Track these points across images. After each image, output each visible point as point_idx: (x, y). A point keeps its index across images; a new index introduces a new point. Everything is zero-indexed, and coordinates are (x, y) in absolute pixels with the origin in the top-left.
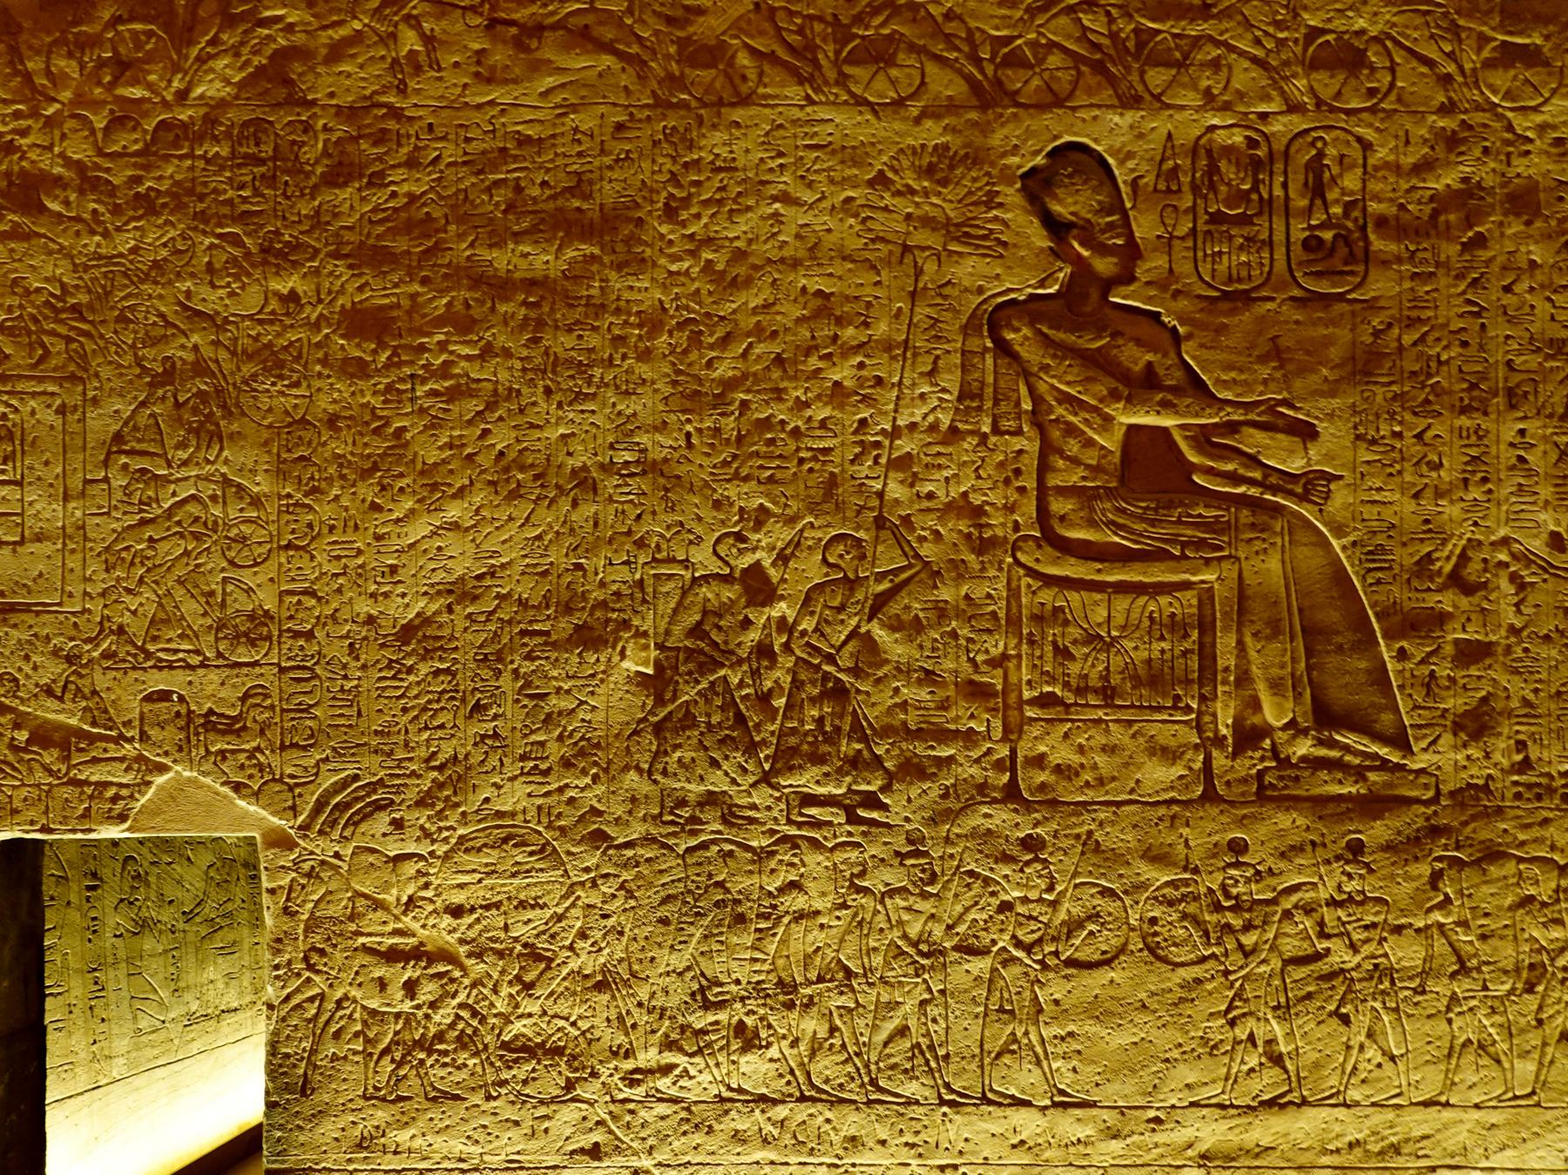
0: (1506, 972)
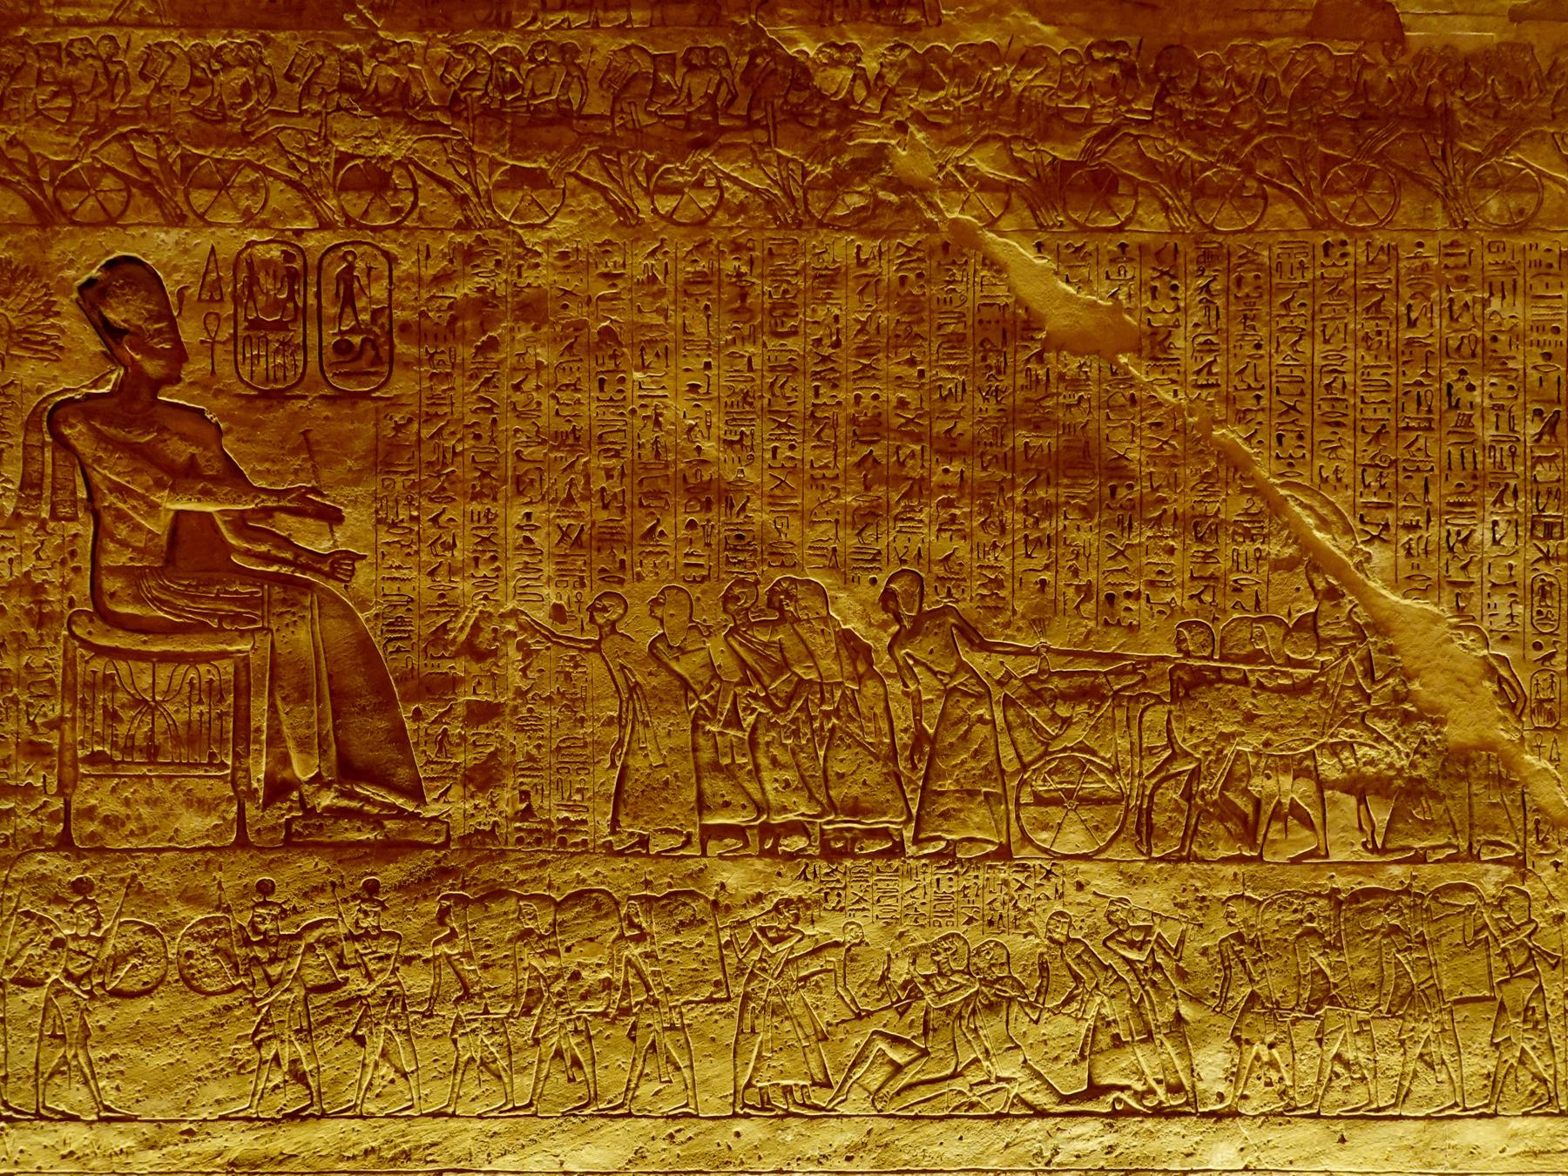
0: (505, 997)
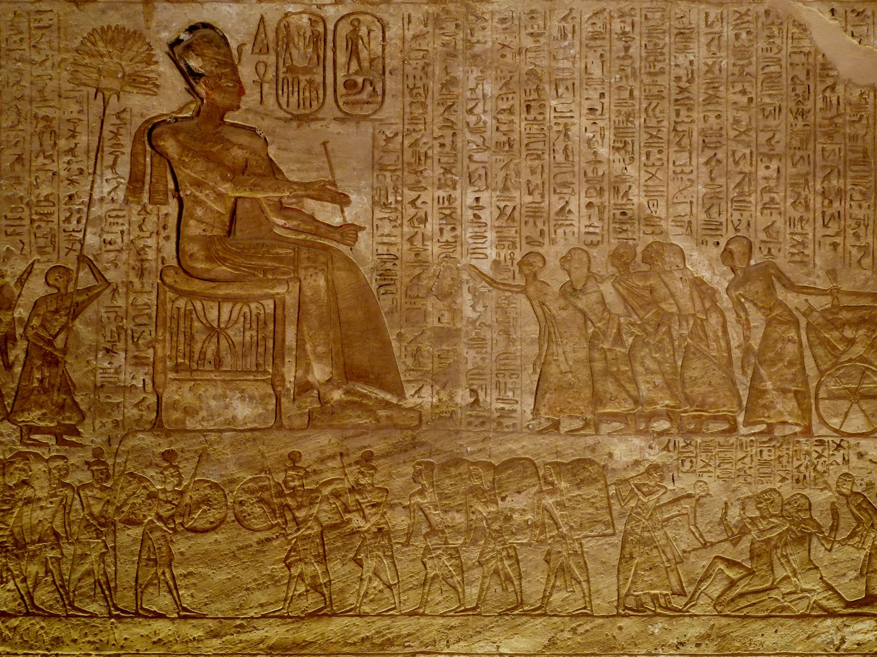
0: (459, 532)
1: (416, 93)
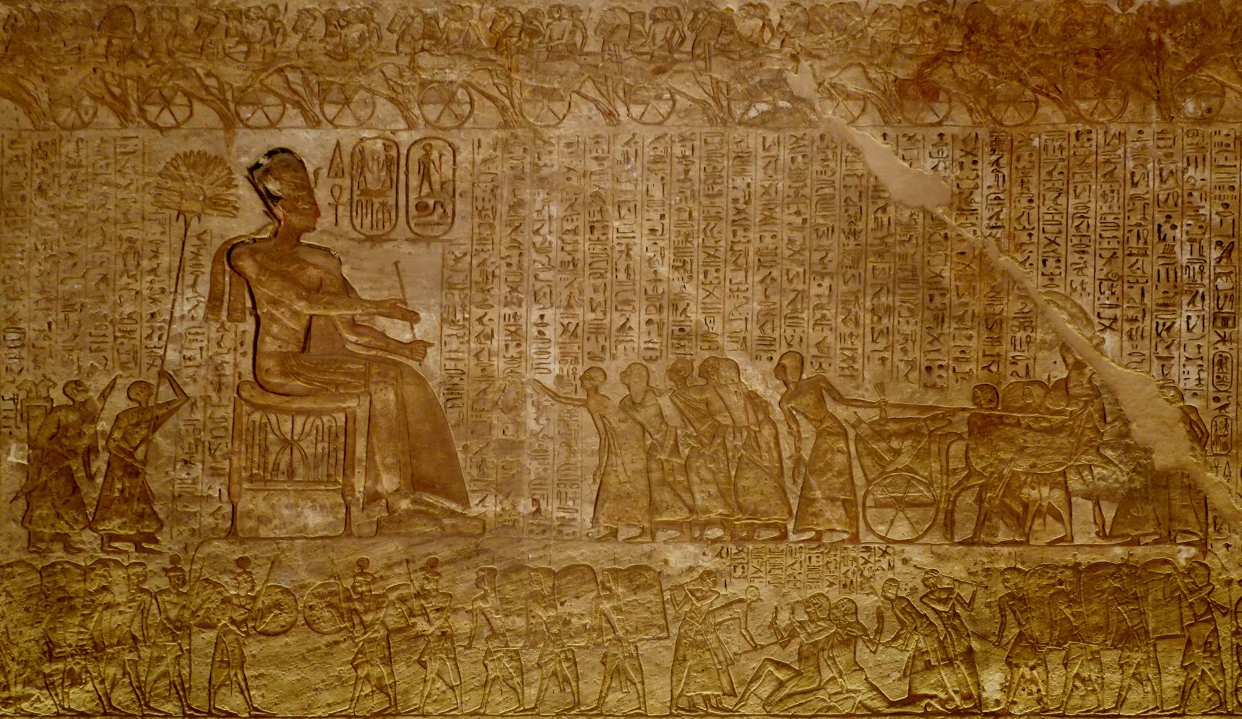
0: (519, 636)
1: (484, 215)
